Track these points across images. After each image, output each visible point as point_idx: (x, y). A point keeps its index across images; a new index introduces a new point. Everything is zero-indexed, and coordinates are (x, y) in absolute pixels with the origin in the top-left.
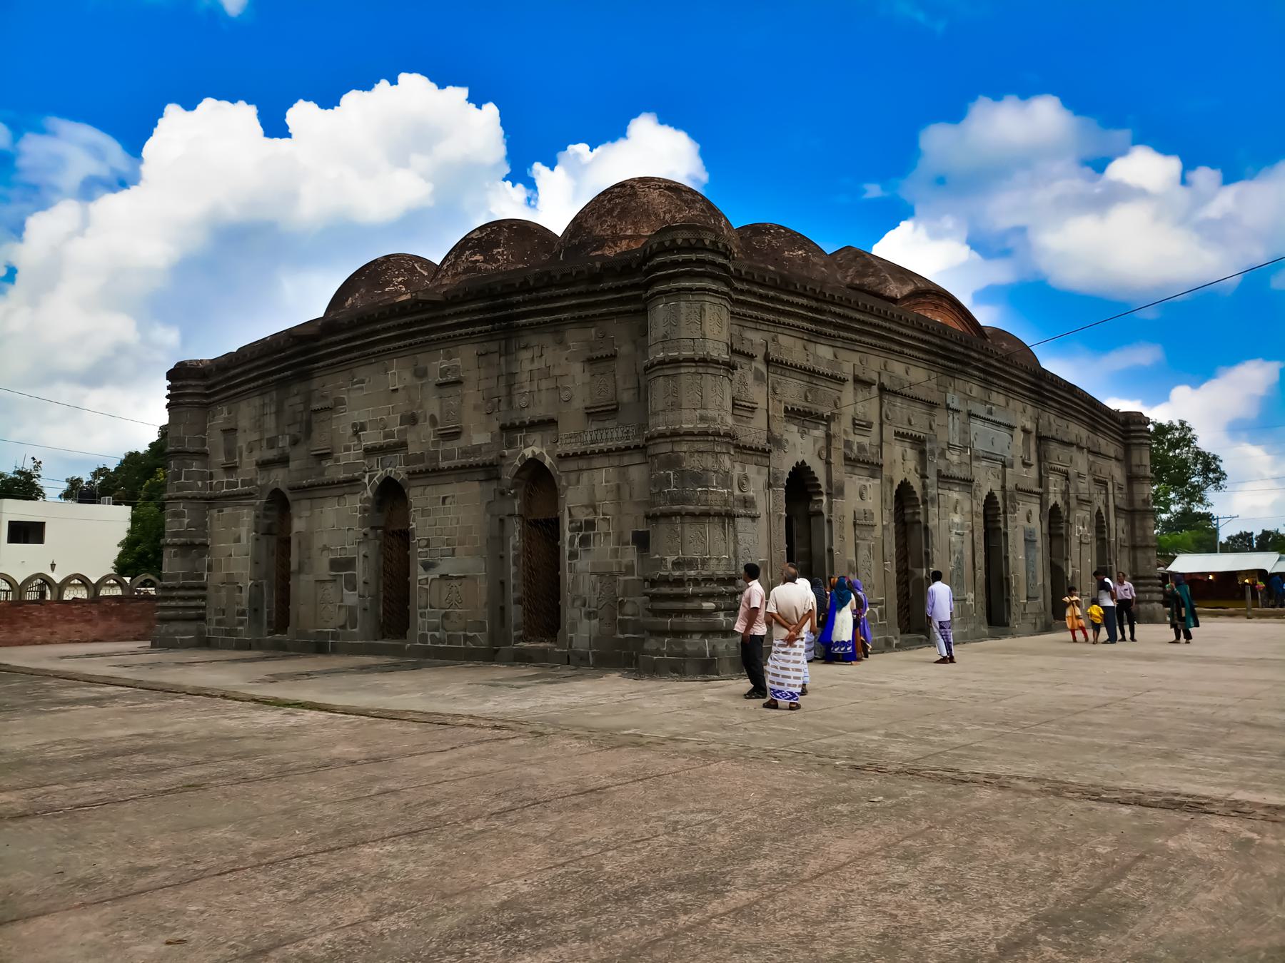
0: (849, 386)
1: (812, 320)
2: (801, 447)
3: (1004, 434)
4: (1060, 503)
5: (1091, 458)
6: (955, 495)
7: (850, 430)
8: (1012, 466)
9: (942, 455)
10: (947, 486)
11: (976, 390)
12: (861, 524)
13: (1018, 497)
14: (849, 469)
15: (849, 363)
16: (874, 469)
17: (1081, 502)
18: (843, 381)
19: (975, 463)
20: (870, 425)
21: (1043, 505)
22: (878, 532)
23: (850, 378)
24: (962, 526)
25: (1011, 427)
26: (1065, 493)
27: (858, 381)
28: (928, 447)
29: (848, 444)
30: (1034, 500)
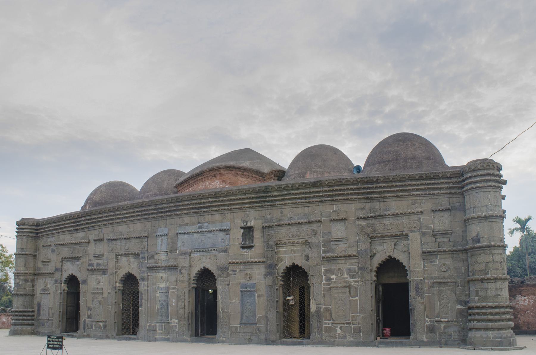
0: (92, 243)
1: (74, 226)
2: (70, 269)
3: (221, 235)
4: (300, 262)
5: (363, 223)
6: (162, 274)
7: (91, 258)
8: (226, 251)
9: (152, 257)
10: (154, 271)
11: (187, 220)
12: (97, 293)
13: (231, 268)
14: (90, 273)
15: (93, 235)
16: (104, 272)
17: (329, 260)
18: (88, 243)
19: (180, 257)
20: (102, 255)
21: (271, 268)
22: (105, 295)
23: (92, 241)
24: (167, 288)
25: (227, 231)
26: (308, 258)
27: (95, 240)
28: (140, 255)
29: (91, 265)
30: (255, 266)
